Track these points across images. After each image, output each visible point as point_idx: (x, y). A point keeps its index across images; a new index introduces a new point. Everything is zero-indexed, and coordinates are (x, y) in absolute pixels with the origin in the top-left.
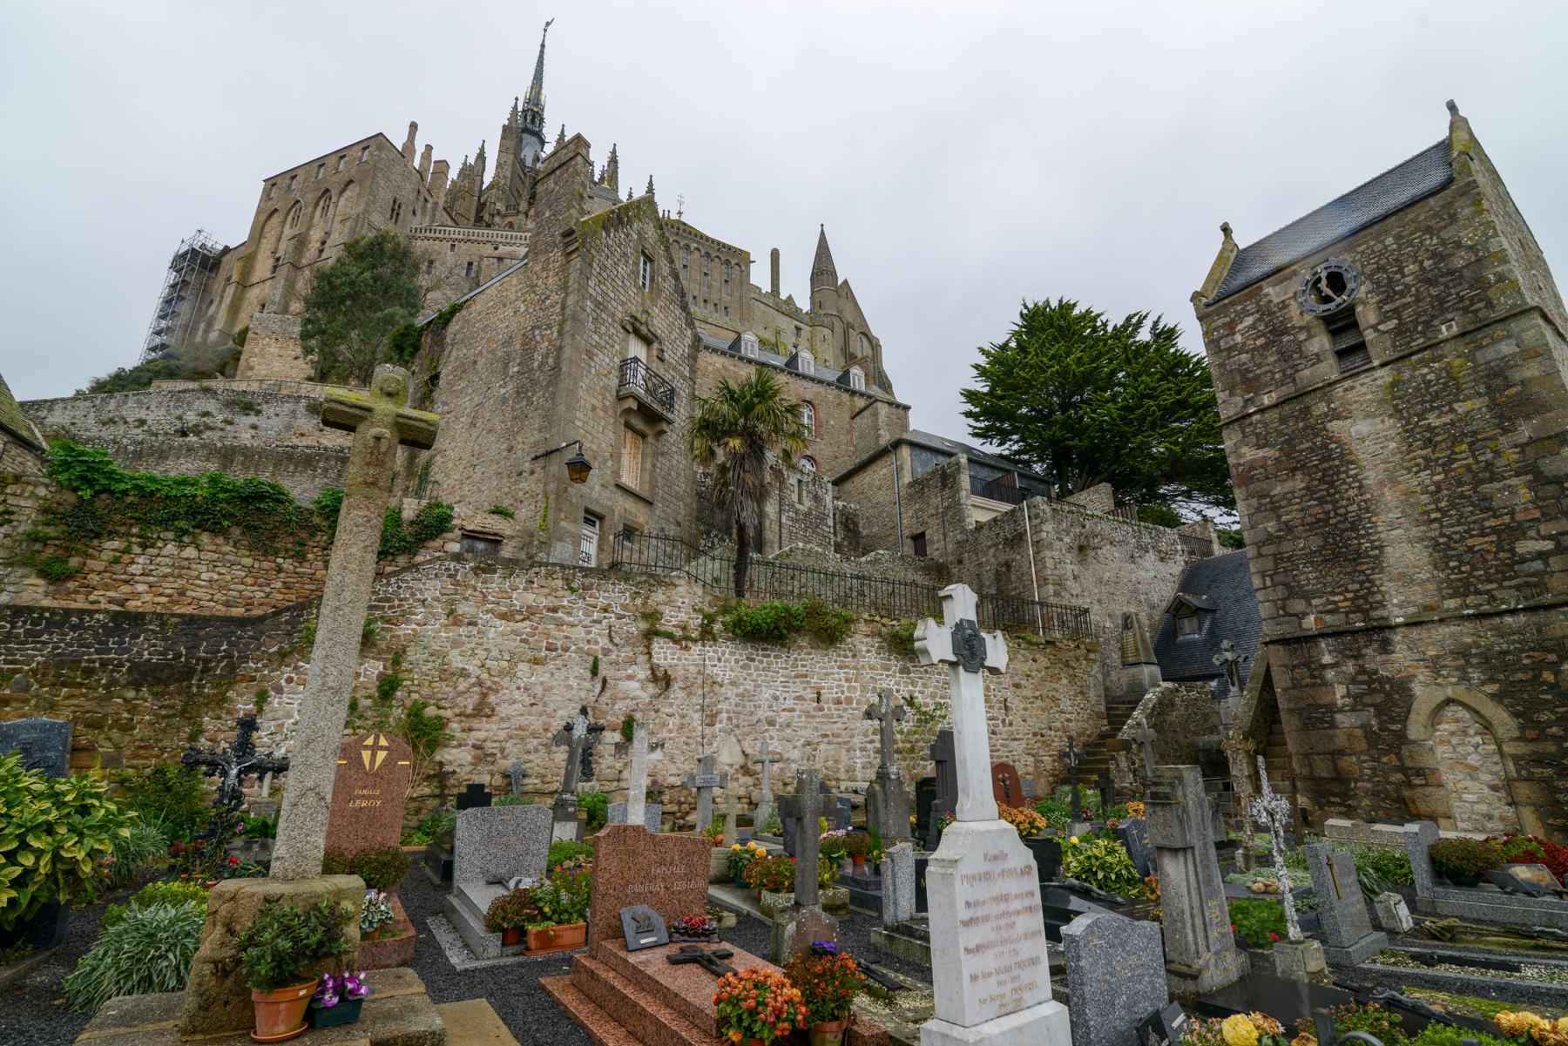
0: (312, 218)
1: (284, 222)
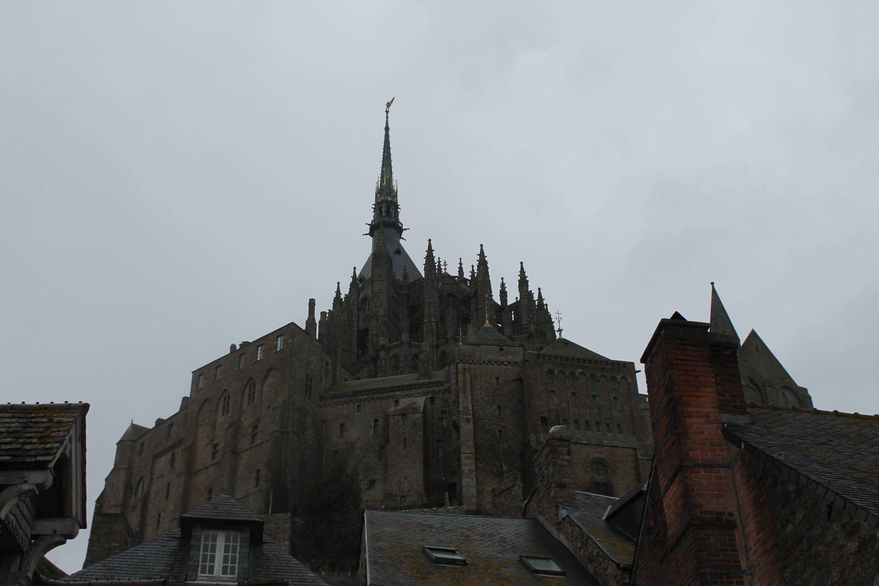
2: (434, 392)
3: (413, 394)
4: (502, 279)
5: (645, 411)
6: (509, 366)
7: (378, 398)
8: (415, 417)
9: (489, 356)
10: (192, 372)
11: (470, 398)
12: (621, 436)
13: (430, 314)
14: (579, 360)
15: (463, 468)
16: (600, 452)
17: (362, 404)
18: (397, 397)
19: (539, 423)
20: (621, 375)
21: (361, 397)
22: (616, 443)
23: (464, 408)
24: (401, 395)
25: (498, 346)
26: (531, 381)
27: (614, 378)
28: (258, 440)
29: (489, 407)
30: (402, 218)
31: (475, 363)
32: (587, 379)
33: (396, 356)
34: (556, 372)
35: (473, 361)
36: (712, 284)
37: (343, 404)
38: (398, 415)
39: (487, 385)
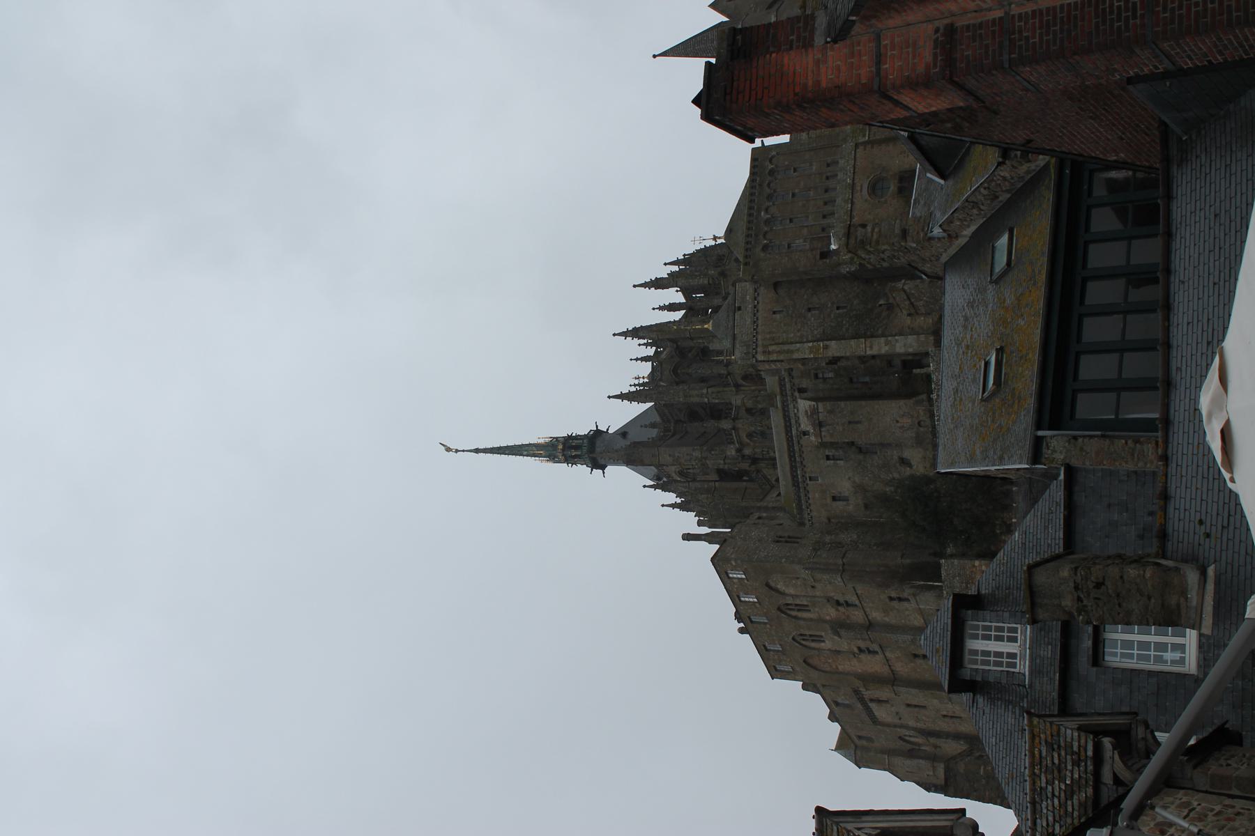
0: (811, 620)
1: (818, 649)
2: (792, 388)
3: (795, 414)
4: (654, 309)
6: (760, 299)
7: (801, 456)
8: (822, 411)
9: (748, 323)
10: (773, 679)
11: (798, 345)
12: (842, 162)
13: (698, 396)
14: (750, 215)
15: (883, 351)
16: (861, 186)
17: (807, 475)
18: (799, 433)
19: (828, 261)
20: (767, 163)
21: (799, 477)
22: (850, 168)
23: (811, 352)
24: (797, 430)
25: (735, 313)
26: (777, 271)
27: (772, 172)
28: (854, 599)
29: (809, 322)
30: (583, 429)
31: (757, 340)
32: (774, 204)
33: (750, 436)
34: (765, 242)
35: (754, 342)
36: (655, 56)
37: (809, 498)
38: (820, 431)
39: (782, 325)
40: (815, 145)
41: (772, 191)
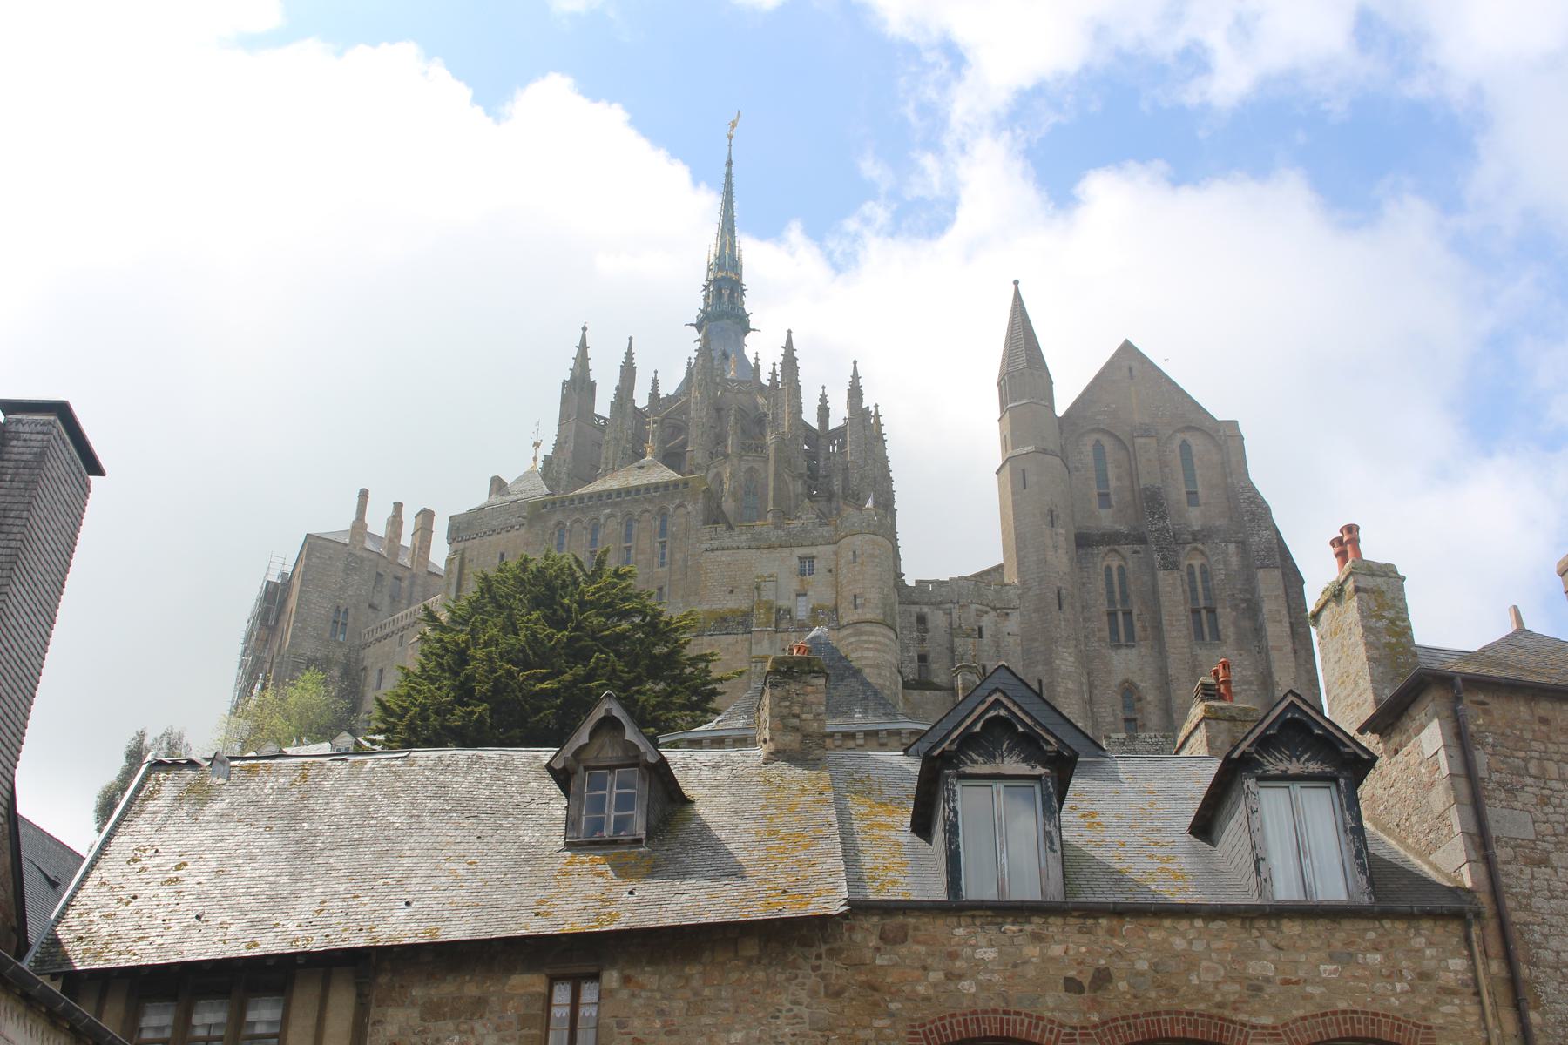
5: (708, 553)
20: (677, 501)
34: (568, 524)
36: (1016, 283)
40: (690, 563)
41: (636, 518)
